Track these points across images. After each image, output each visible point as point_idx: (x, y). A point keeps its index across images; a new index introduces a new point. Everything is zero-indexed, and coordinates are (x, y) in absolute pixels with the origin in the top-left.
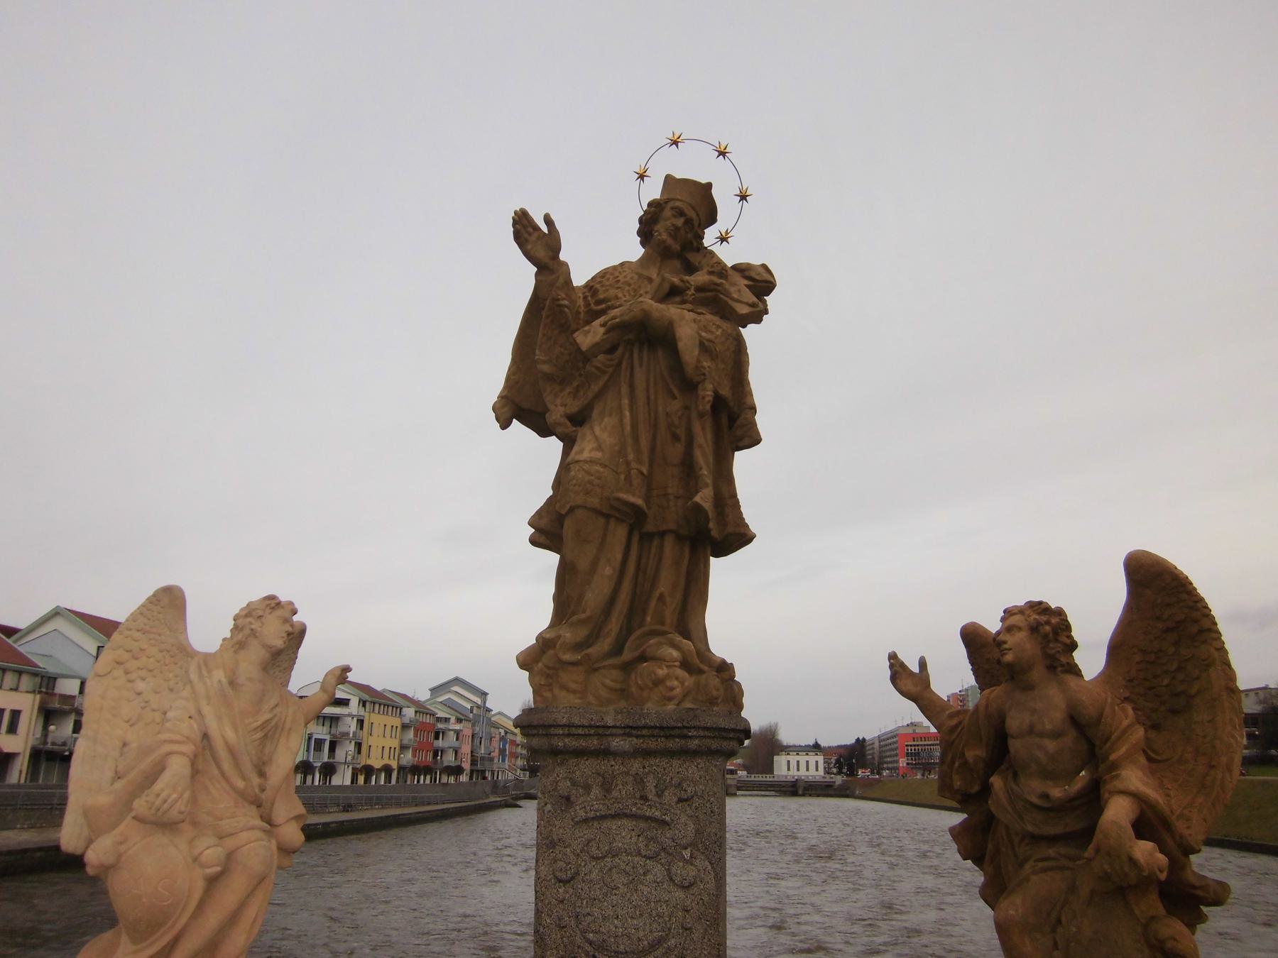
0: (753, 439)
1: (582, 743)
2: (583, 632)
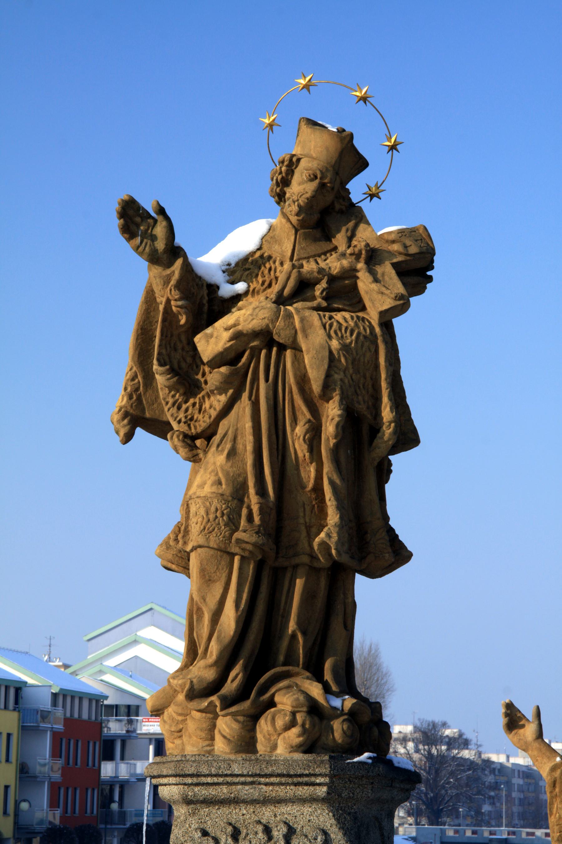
0: (407, 438)
1: (212, 792)
2: (210, 675)
